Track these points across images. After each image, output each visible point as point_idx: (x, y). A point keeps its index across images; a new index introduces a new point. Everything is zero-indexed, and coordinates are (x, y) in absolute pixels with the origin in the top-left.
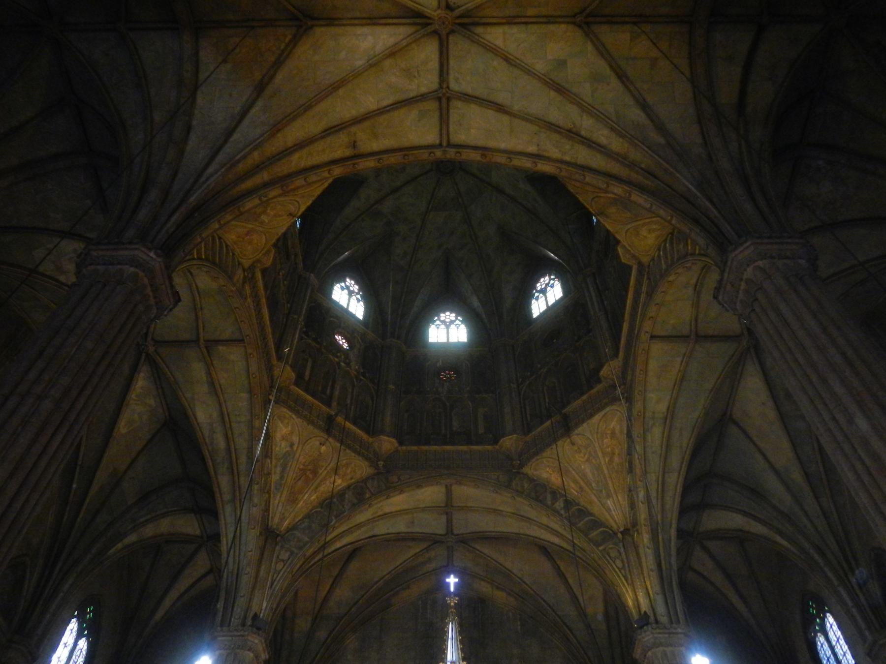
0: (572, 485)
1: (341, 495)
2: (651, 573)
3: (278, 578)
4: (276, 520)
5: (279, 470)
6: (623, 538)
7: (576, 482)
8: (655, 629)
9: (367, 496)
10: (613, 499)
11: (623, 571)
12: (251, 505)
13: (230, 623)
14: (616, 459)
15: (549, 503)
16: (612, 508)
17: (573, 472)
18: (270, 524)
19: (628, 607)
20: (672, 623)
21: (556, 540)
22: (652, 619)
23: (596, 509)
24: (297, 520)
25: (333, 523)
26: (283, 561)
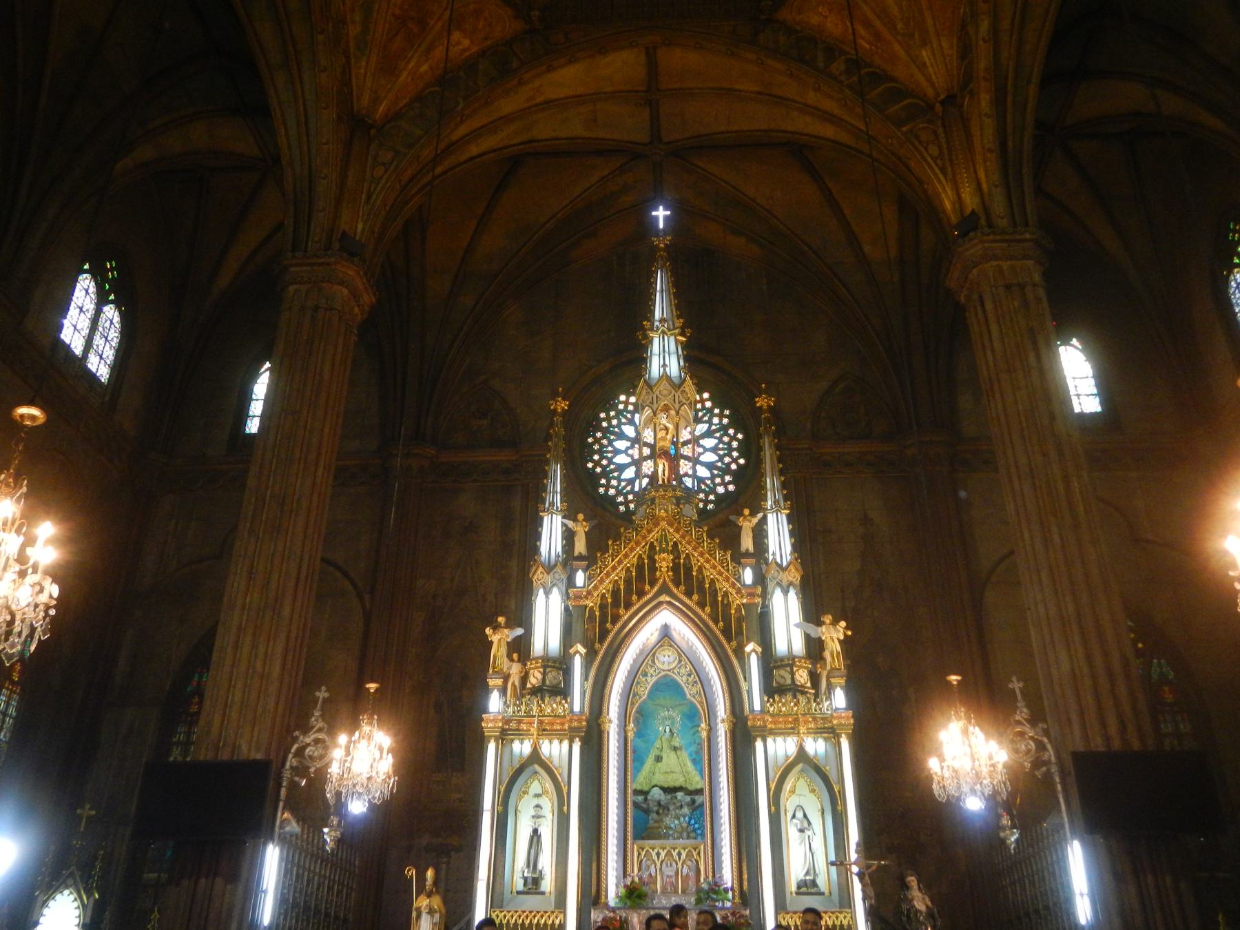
0: (861, 31)
2: (988, 155)
3: (377, 192)
4: (365, 101)
5: (358, 18)
6: (943, 111)
7: (867, 24)
8: (988, 235)
9: (514, 65)
10: (932, 47)
11: (939, 162)
12: (317, 69)
13: (306, 247)
15: (821, 64)
16: (928, 64)
17: (865, 8)
18: (355, 109)
19: (944, 212)
20: (1015, 225)
21: (829, 131)
22: (983, 222)
24: (401, 105)
25: (459, 108)
26: (384, 164)
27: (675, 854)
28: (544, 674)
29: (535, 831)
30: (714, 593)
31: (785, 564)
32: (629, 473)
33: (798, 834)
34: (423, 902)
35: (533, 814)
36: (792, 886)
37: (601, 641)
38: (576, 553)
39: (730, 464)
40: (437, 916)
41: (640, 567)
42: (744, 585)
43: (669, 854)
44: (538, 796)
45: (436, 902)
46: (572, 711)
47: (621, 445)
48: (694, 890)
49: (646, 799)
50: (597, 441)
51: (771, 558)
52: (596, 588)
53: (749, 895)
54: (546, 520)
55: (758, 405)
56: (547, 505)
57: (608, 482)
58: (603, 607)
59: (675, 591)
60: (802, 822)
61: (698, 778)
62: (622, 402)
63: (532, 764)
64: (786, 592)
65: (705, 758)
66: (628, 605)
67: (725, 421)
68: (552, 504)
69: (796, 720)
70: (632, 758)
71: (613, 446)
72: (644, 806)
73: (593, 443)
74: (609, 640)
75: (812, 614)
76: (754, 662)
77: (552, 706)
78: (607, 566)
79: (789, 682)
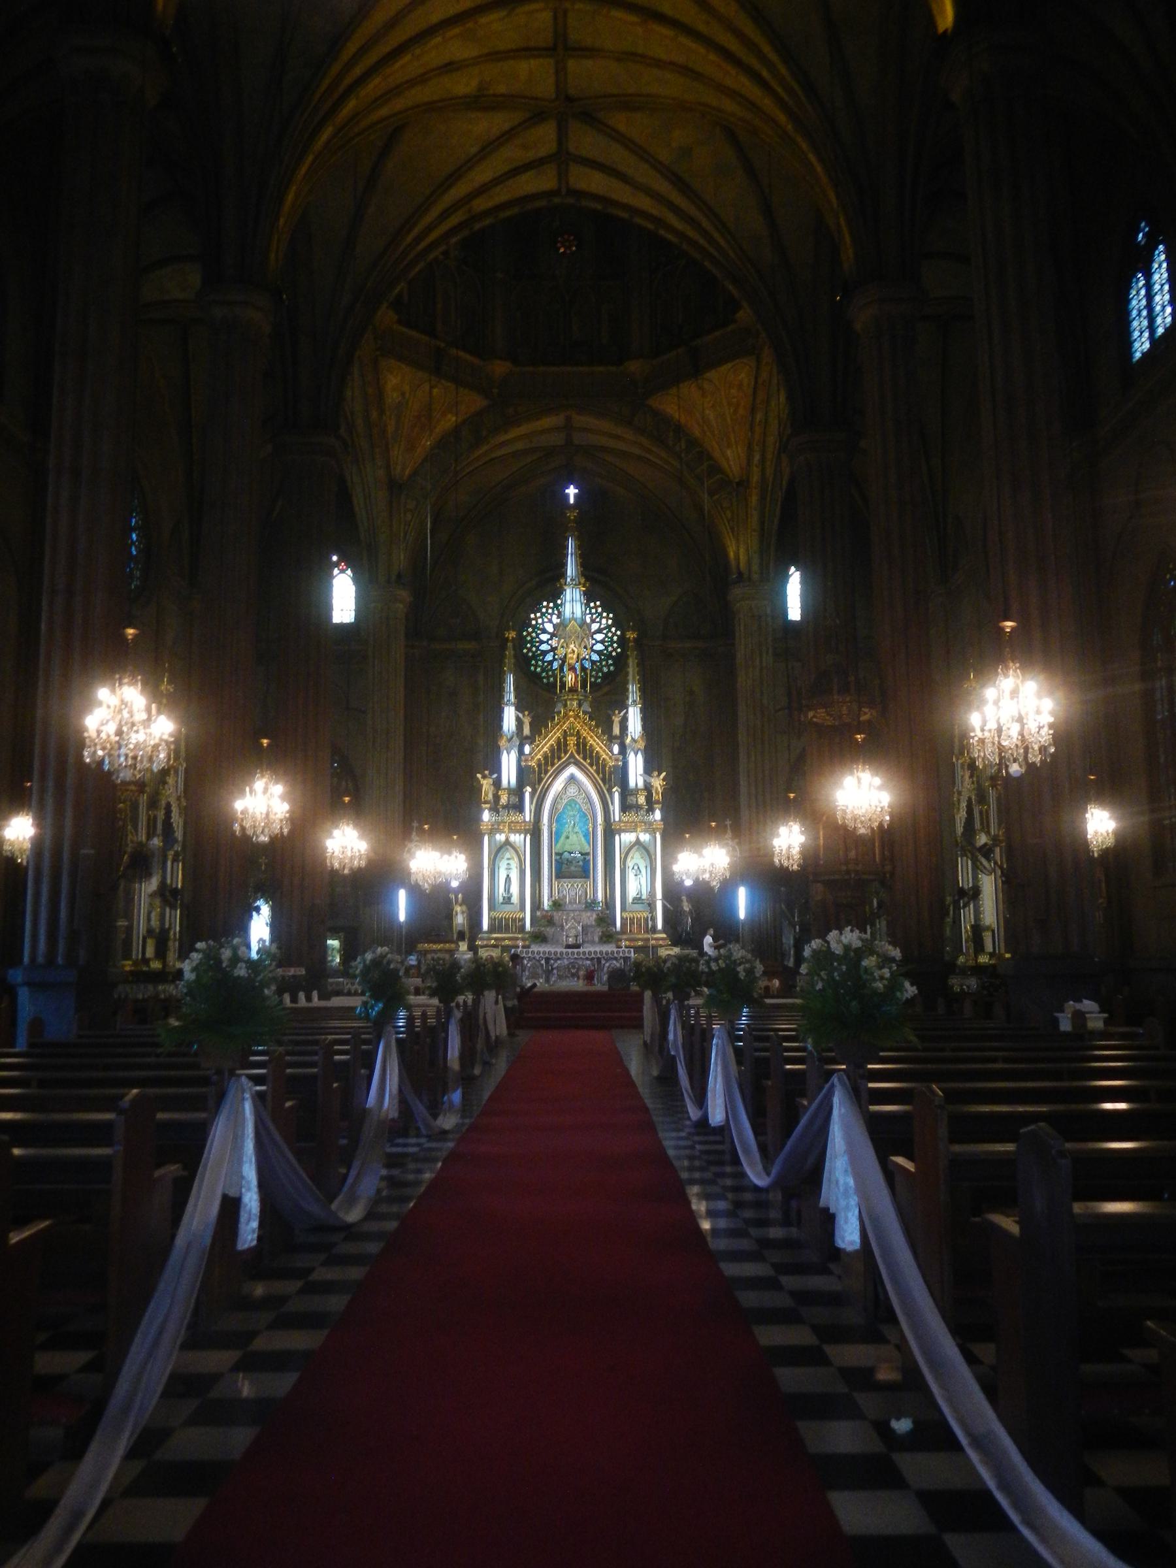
1: (456, 431)
14: (741, 411)
16: (730, 458)
23: (717, 454)
27: (575, 886)
28: (509, 798)
29: (508, 876)
30: (598, 756)
31: (636, 738)
32: (549, 657)
33: (634, 877)
34: (458, 909)
35: (506, 867)
36: (630, 900)
37: (540, 782)
38: (525, 734)
39: (611, 652)
40: (465, 915)
41: (558, 742)
42: (613, 754)
43: (572, 885)
44: (508, 859)
45: (464, 908)
46: (525, 821)
47: (544, 637)
48: (584, 901)
49: (561, 858)
50: (529, 634)
51: (629, 734)
52: (536, 755)
53: (609, 904)
54: (506, 709)
55: (628, 636)
56: (506, 700)
57: (537, 662)
58: (539, 765)
59: (577, 757)
60: (636, 872)
61: (587, 847)
62: (544, 607)
63: (506, 845)
64: (636, 754)
65: (590, 837)
66: (553, 765)
67: (610, 622)
68: (509, 701)
69: (636, 825)
70: (554, 836)
71: (538, 638)
72: (560, 861)
73: (527, 636)
74: (543, 783)
75: (648, 771)
76: (617, 796)
77: (515, 817)
78: (541, 743)
79: (635, 803)
